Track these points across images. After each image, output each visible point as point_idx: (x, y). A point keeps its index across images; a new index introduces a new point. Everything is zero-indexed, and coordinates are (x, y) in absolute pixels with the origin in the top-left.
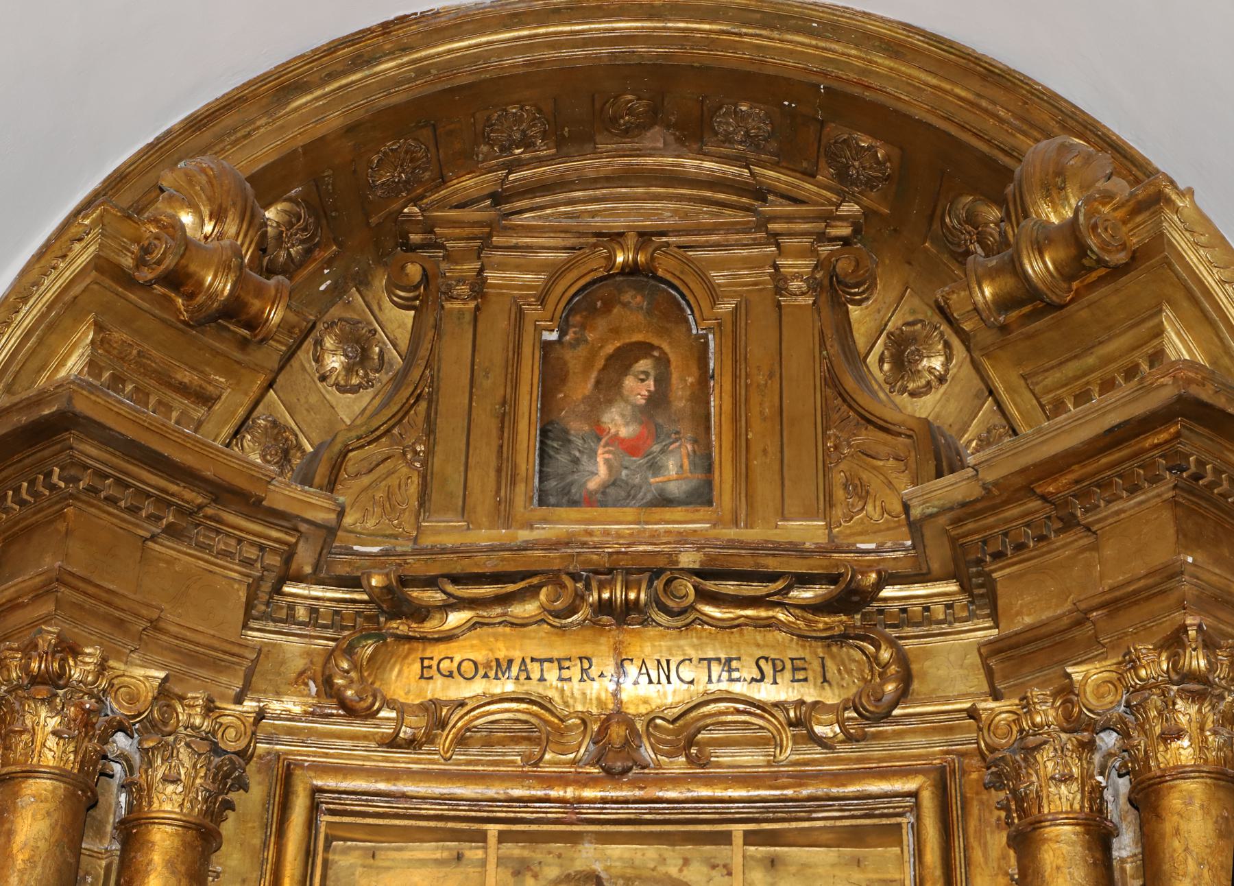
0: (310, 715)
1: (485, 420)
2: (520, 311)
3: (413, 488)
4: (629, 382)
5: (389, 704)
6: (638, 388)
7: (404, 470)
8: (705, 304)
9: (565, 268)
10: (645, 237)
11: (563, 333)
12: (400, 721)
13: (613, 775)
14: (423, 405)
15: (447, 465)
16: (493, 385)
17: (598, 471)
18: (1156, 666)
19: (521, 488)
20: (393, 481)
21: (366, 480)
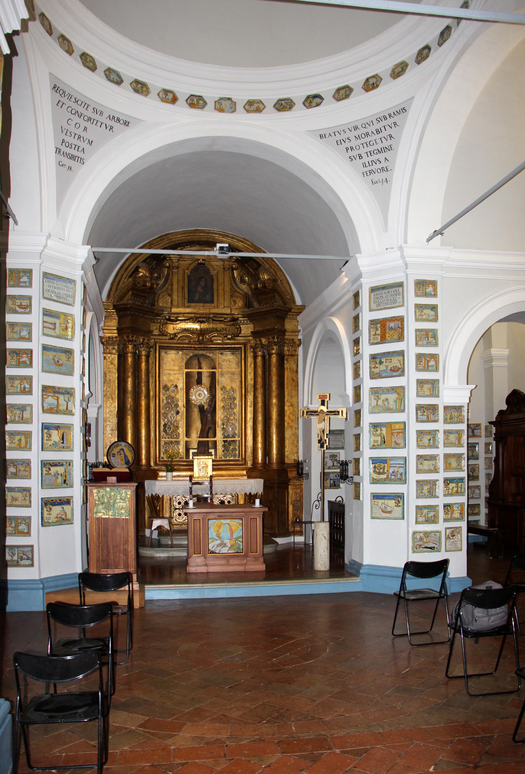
0: (159, 335)
1: (180, 289)
2: (184, 271)
3: (170, 300)
4: (201, 282)
5: (169, 333)
6: (202, 283)
7: (168, 297)
8: (213, 271)
9: (191, 264)
10: (203, 260)
11: (191, 274)
12: (170, 335)
13: (200, 344)
14: (170, 286)
15: (175, 297)
16: (181, 284)
17: (197, 298)
18: (271, 340)
19: (186, 300)
20: (167, 299)
21: (163, 299)
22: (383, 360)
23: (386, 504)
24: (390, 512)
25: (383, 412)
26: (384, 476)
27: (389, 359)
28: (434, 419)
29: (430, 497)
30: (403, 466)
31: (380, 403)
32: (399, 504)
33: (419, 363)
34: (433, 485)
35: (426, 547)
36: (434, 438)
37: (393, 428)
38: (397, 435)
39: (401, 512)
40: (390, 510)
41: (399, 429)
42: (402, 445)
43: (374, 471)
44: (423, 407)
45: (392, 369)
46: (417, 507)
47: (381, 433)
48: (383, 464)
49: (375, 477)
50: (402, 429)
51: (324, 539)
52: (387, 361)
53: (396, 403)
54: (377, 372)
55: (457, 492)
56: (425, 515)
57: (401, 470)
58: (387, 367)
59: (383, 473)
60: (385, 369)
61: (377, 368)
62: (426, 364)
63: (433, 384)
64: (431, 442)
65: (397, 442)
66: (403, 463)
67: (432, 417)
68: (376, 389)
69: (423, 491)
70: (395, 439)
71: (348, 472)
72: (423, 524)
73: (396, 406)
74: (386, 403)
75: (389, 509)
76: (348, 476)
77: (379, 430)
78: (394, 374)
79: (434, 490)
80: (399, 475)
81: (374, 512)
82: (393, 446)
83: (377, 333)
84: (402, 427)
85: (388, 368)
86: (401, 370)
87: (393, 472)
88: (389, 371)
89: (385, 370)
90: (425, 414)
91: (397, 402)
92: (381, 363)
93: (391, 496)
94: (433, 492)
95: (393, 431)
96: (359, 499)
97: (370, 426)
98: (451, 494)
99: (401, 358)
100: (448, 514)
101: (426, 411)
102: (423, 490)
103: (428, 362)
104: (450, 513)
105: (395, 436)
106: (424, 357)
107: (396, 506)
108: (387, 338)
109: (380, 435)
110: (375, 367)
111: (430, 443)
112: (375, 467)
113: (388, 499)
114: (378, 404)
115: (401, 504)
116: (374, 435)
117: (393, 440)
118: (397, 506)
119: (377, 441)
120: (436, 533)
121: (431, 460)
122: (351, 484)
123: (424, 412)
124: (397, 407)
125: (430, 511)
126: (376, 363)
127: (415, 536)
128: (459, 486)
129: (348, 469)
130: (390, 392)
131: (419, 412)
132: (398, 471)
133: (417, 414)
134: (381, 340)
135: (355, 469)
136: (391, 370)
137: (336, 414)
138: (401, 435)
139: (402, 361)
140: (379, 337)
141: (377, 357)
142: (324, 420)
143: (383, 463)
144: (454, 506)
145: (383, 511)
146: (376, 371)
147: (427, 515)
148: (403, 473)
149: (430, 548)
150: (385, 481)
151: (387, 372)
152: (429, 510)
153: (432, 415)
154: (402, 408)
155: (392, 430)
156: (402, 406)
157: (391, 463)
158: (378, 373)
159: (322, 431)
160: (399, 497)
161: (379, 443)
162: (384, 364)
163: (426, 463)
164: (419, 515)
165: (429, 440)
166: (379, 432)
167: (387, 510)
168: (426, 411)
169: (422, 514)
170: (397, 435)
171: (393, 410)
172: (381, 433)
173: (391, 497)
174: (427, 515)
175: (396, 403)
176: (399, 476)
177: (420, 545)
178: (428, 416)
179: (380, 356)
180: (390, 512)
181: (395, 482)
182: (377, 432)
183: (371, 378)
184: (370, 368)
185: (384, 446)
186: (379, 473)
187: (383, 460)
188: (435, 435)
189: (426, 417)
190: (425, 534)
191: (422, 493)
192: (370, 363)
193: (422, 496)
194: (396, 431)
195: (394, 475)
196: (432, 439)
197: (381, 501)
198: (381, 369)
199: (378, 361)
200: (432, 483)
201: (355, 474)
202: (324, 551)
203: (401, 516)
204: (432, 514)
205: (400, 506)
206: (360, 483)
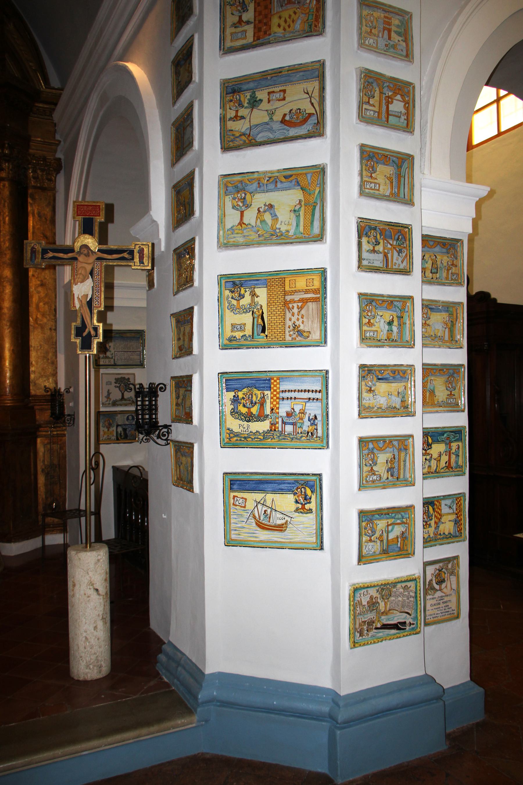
22: (261, 95)
23: (269, 503)
24: (280, 528)
25: (259, 244)
26: (264, 426)
27: (277, 89)
28: (402, 267)
29: (394, 486)
30: (318, 395)
31: (250, 217)
32: (307, 506)
33: (366, 99)
34: (400, 450)
35: (385, 627)
36: (400, 318)
37: (287, 288)
38: (300, 308)
39: (313, 529)
40: (279, 522)
41: (307, 292)
42: (316, 336)
43: (234, 412)
44: (375, 229)
45: (287, 118)
46: (363, 515)
47: (253, 304)
48: (259, 393)
49: (236, 429)
50: (315, 291)
51: (94, 596)
52: (274, 97)
53: (298, 217)
54: (243, 130)
55: (449, 466)
56: (381, 536)
57: (313, 409)
58: (271, 114)
59: (262, 417)
60: (267, 119)
61: (242, 118)
62: (384, 108)
63: (399, 167)
64: (395, 329)
65: (302, 328)
66: (318, 389)
67: (396, 260)
68: (238, 178)
69: (375, 468)
70: (294, 319)
71: (156, 414)
72: (378, 560)
73: (298, 225)
74: (267, 217)
75: (277, 519)
76: (157, 422)
77: (247, 295)
78: (293, 132)
79: (402, 463)
80: (307, 423)
81: (233, 525)
82: (288, 338)
83: (245, 17)
84: (317, 284)
85: (275, 118)
86: (313, 120)
87: (289, 415)
88: (276, 126)
89: (267, 124)
90: (380, 248)
91: (302, 213)
92: (254, 103)
93: (283, 482)
94: (399, 469)
95: (288, 298)
96: (191, 489)
97: (219, 284)
98: (436, 472)
99: (313, 86)
100: (430, 525)
101: (381, 241)
102: (376, 464)
103: (389, 102)
104: (432, 523)
105: (295, 310)
106: (378, 85)
107: (297, 510)
108: (275, 28)
109: (251, 309)
110: (236, 118)
111: (390, 331)
112: (235, 400)
113: (274, 491)
114: (245, 221)
115: (312, 505)
116: (232, 309)
117: (289, 323)
118: (302, 510)
119: (242, 327)
120: (409, 584)
121: (395, 379)
122: (163, 442)
123: (378, 243)
124: (301, 229)
125: (393, 524)
126: (241, 105)
127: (357, 599)
128: (453, 451)
129: (156, 405)
130: (279, 185)
131: (364, 240)
132: (303, 412)
133: (360, 244)
134: (256, 37)
135: (177, 404)
136: (283, 121)
137: (123, 259)
138: (312, 306)
139: (316, 94)
140: (250, 30)
141: (245, 87)
142: (91, 273)
143: (258, 388)
144: (443, 503)
145: (261, 526)
146: (240, 126)
147: (385, 535)
148: (319, 418)
149: (395, 626)
150: (265, 438)
151: (271, 130)
152: (390, 521)
153: (396, 254)
154: (316, 230)
155: (285, 293)
156: (317, 224)
157: (282, 388)
158: (244, 134)
159: (84, 302)
160: (306, 484)
161: (248, 331)
162: (264, 105)
163: (382, 387)
164: (365, 538)
165: (390, 323)
166: (246, 300)
167: (272, 523)
168: (381, 241)
169: (374, 532)
170: (300, 308)
171: (288, 237)
172: (253, 304)
173: (282, 486)
174: (385, 535)
175: (298, 217)
176: (306, 426)
177: (371, 623)
178: (386, 256)
179: (252, 85)
180: (280, 528)
181: (293, 444)
182: (243, 302)
183: (226, 148)
184: (223, 120)
185: (261, 338)
186: (249, 418)
187: (258, 380)
188: (403, 310)
189: (381, 256)
190: (383, 589)
191: (374, 474)
192: (223, 106)
193: (373, 481)
194: (297, 297)
195: (294, 424)
196: (396, 323)
197: (252, 497)
198: (254, 122)
199: (246, 97)
200: (395, 443)
201: (177, 419)
202: (95, 628)
203: (314, 539)
204: (397, 531)
205: (310, 511)
206: (192, 445)
